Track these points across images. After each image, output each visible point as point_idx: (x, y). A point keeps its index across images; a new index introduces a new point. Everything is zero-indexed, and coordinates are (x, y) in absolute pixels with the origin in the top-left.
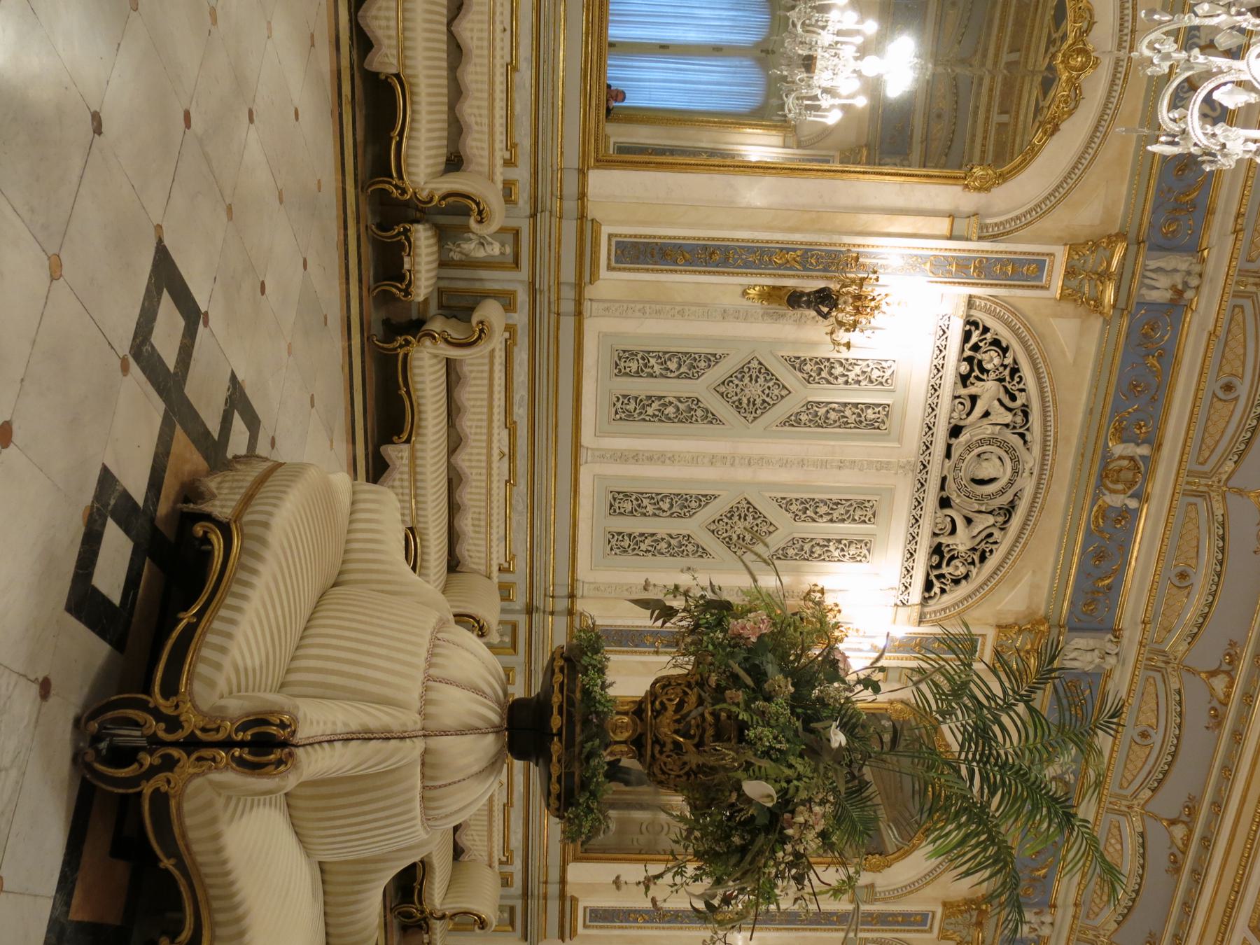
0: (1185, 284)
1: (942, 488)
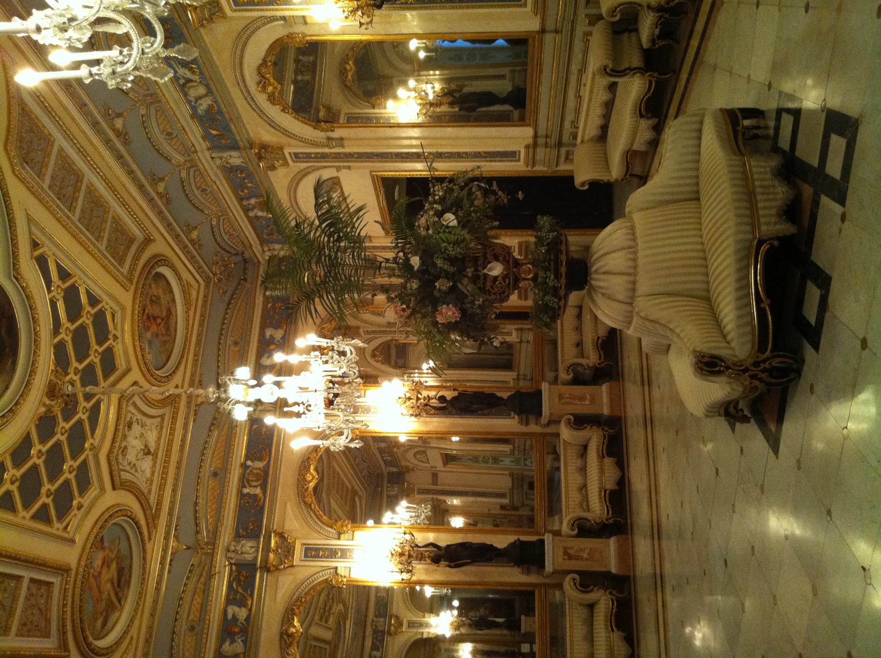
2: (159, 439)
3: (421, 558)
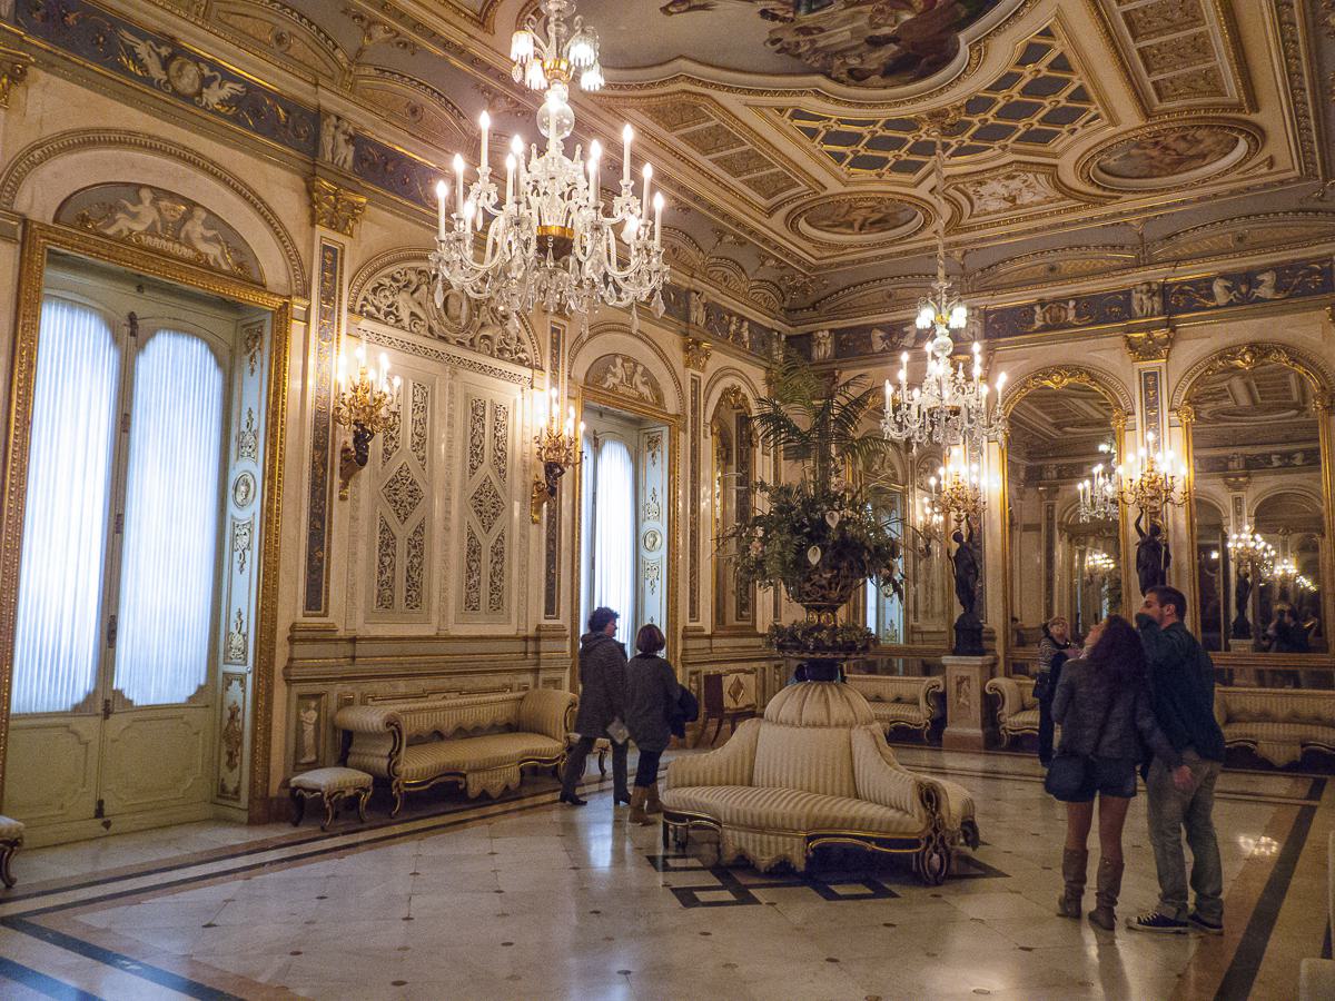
0: (344, 133)
1: (462, 344)
2: (1039, 204)
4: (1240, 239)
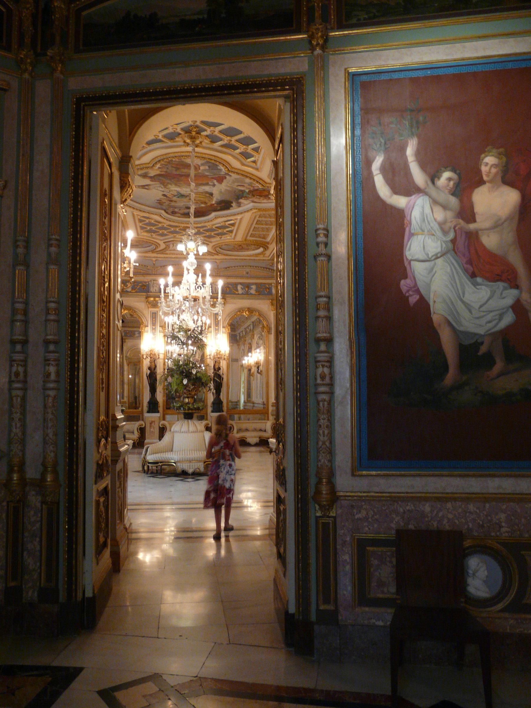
3: (151, 362)
4: (247, 273)
